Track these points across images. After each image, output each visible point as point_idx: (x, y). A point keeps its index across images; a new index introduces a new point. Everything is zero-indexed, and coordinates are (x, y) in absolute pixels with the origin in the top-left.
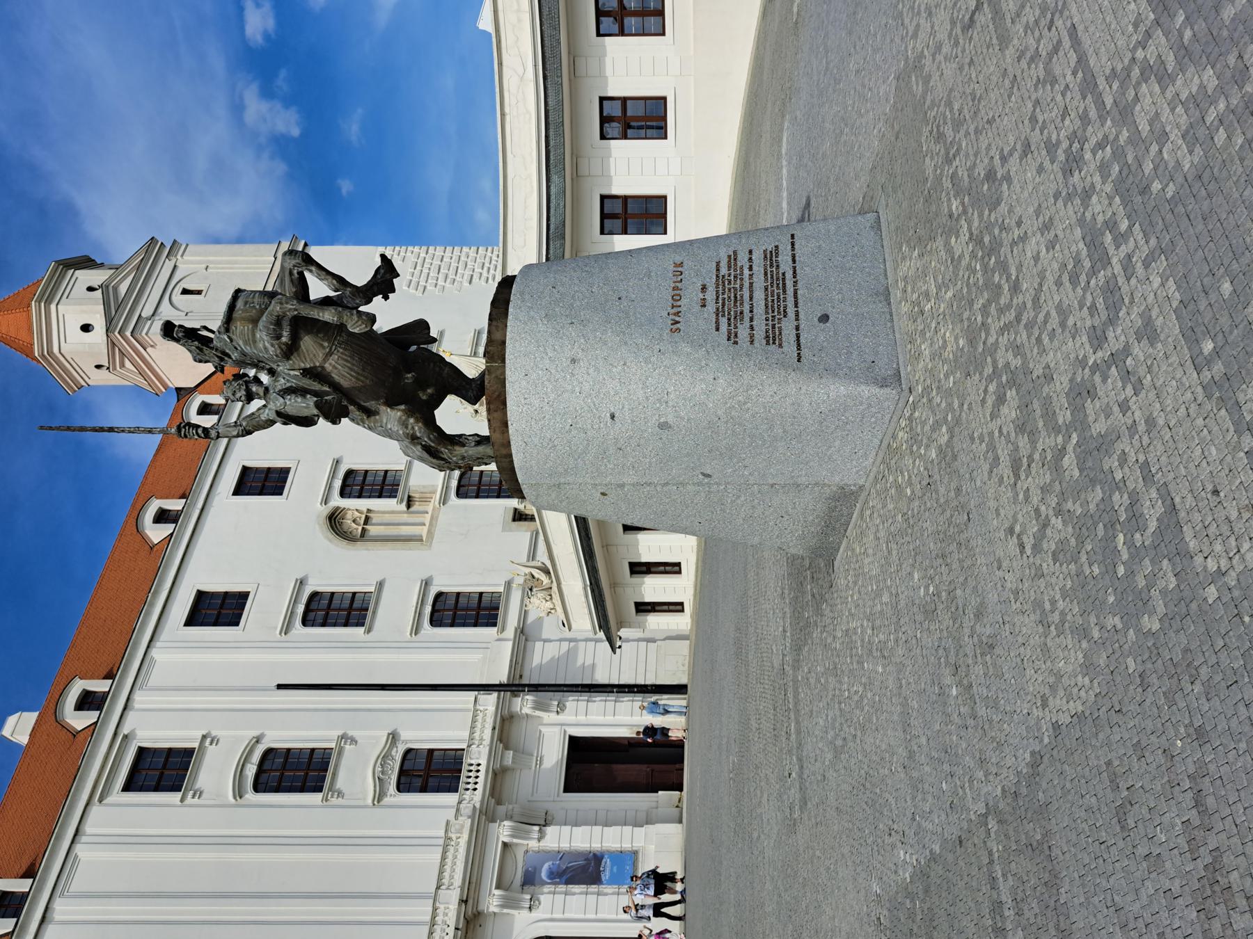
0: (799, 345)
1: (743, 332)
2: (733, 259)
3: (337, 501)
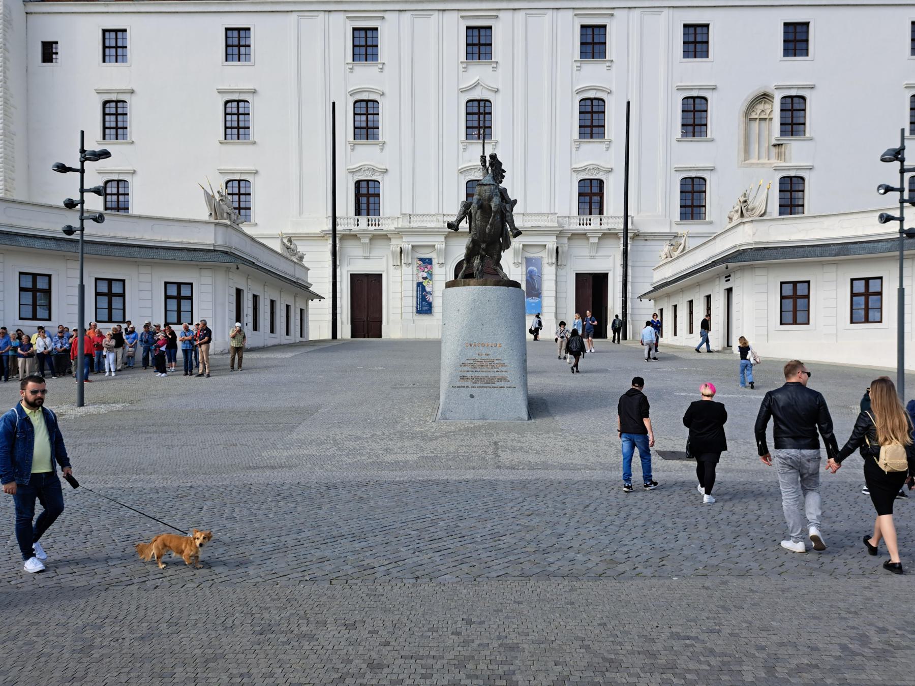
3: (778, 96)
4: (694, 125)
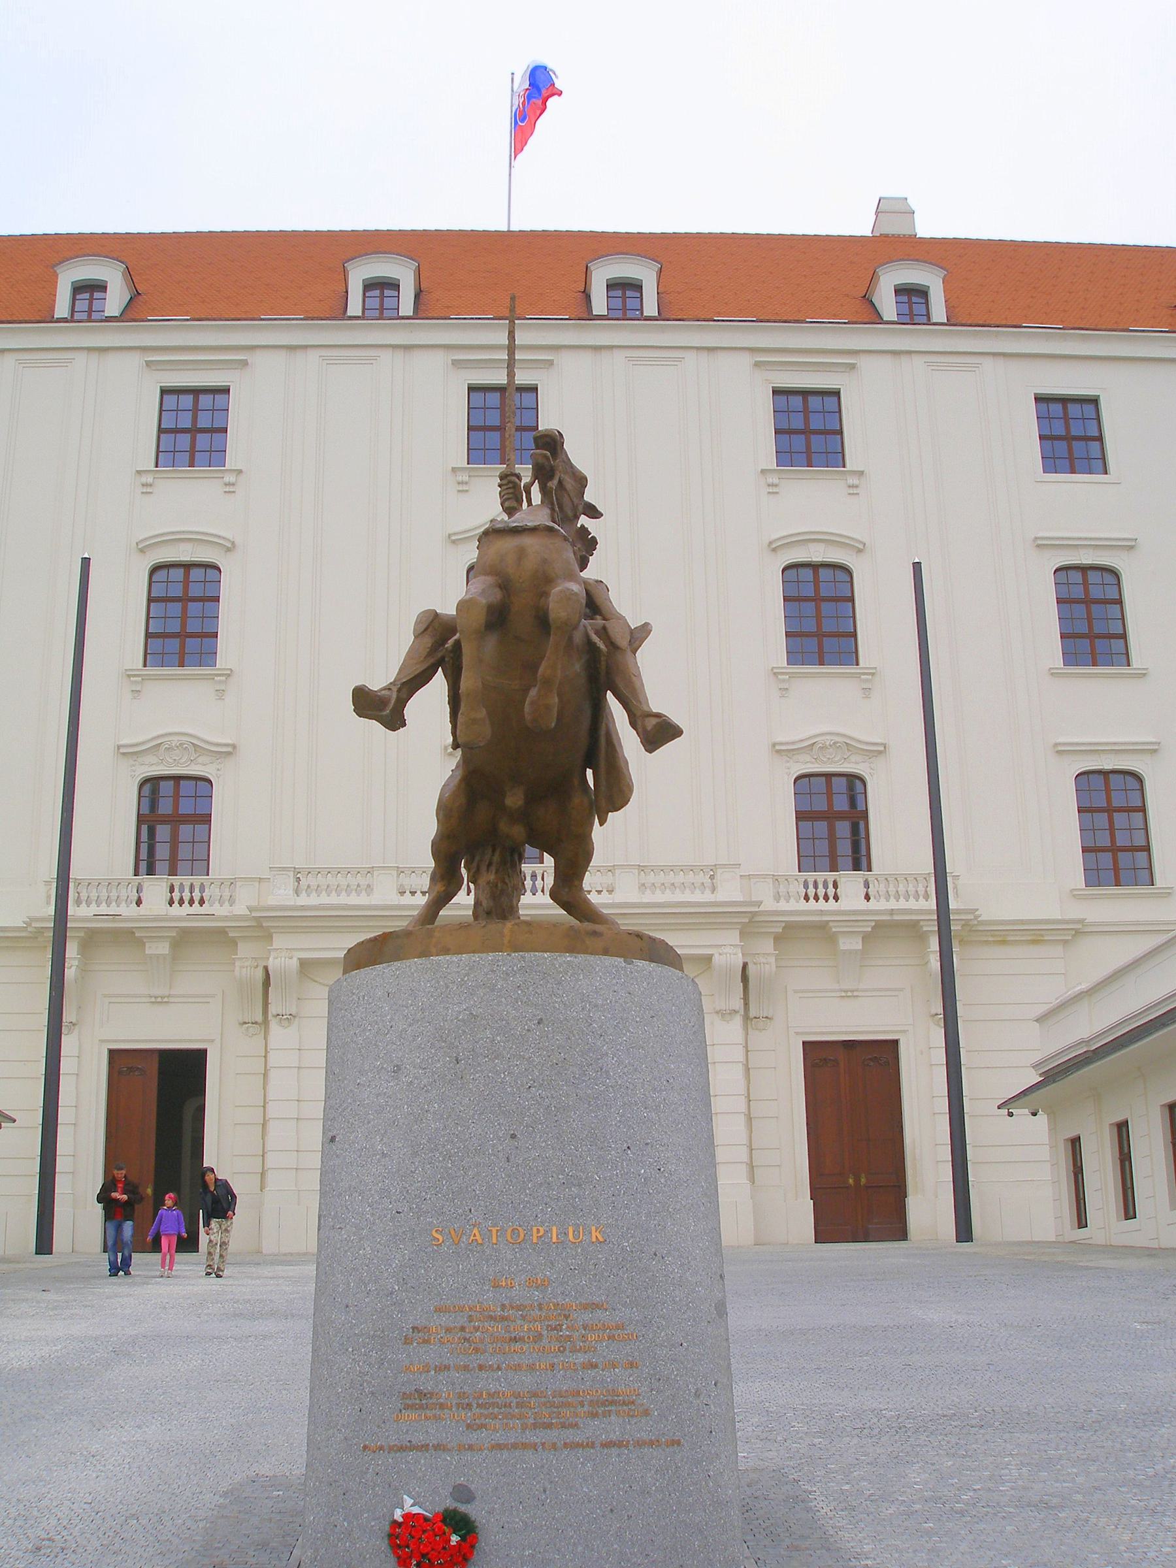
0: (402, 1449)
4: (1092, 636)
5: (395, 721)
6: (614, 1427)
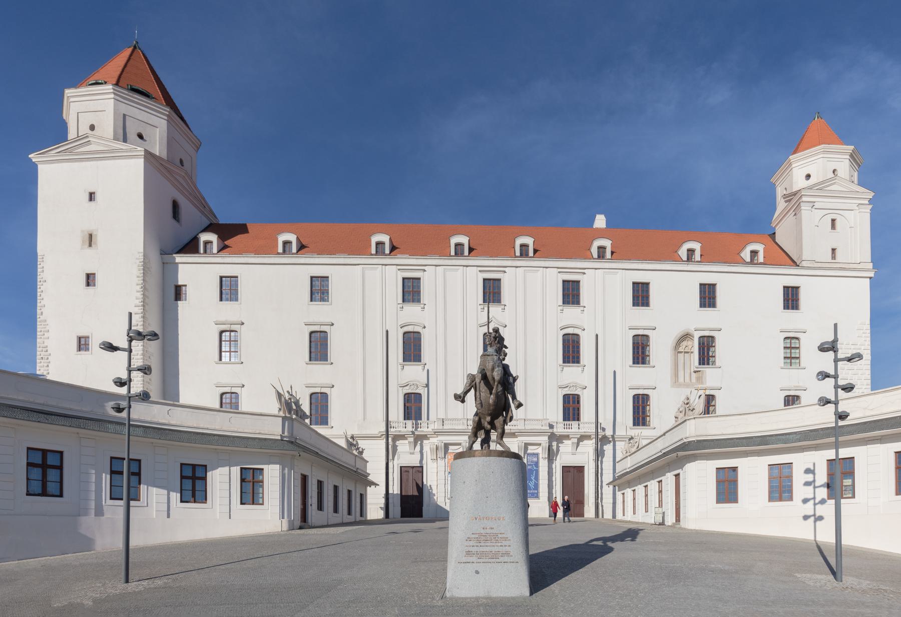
1: (471, 543)
2: (506, 539)
3: (697, 335)
5: (463, 401)
6: (506, 559)
